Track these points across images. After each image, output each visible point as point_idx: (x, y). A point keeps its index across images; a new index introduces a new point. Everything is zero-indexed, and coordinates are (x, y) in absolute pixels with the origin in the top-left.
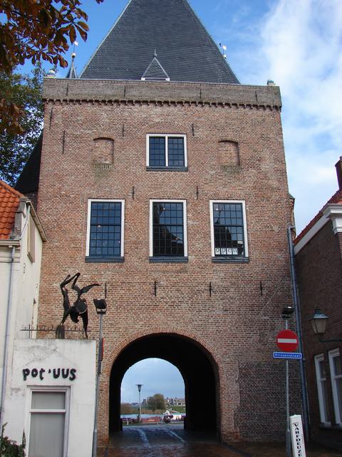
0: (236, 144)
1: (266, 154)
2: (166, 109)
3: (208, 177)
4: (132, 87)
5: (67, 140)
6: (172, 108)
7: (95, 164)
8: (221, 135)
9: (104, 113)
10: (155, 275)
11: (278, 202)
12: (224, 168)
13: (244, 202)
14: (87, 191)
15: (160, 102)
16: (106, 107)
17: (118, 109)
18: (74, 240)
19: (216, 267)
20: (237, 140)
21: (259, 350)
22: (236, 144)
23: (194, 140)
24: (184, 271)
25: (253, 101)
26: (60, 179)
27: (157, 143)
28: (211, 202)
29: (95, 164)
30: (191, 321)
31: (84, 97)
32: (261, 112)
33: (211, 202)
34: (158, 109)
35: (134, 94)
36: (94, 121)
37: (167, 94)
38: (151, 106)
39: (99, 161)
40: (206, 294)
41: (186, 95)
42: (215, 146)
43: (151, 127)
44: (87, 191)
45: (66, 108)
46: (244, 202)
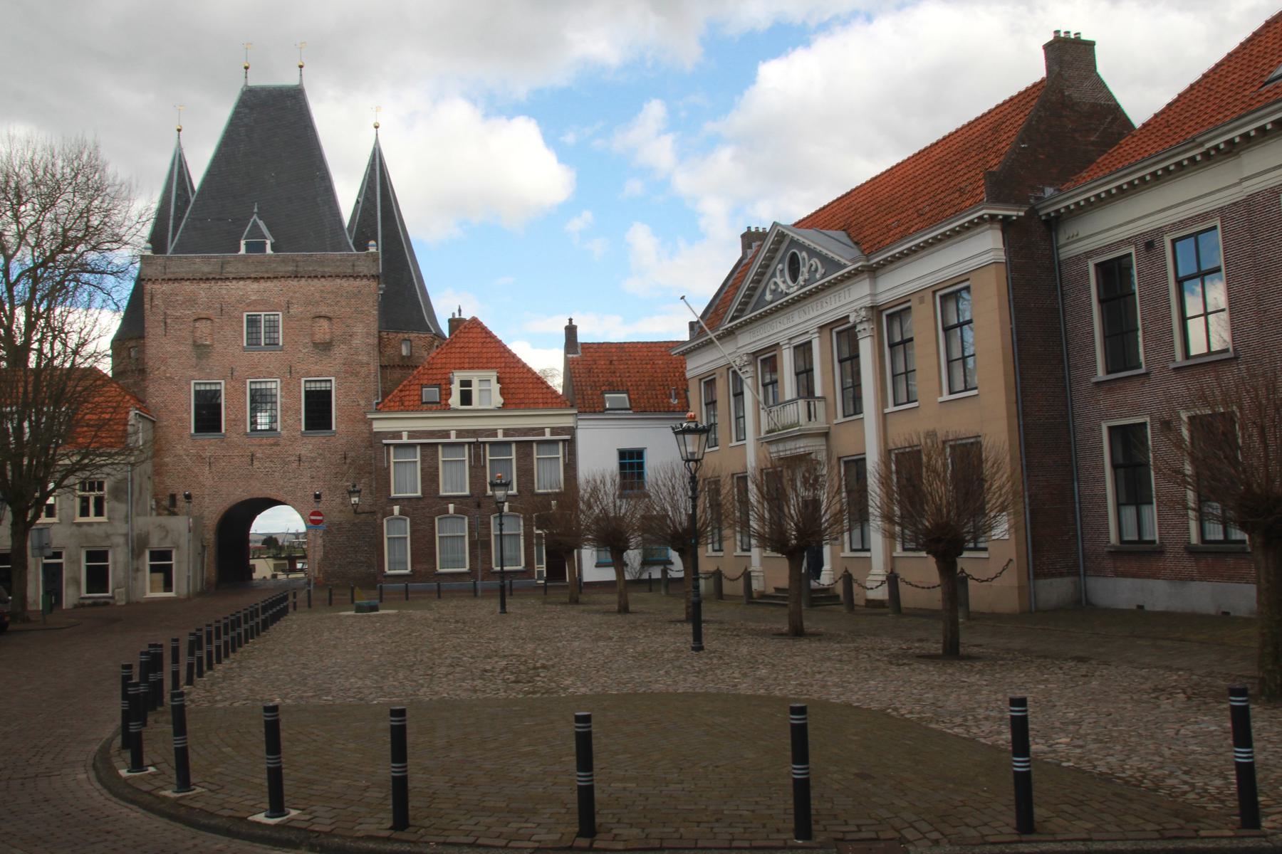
0: (330, 319)
1: (359, 329)
2: (263, 285)
3: (301, 355)
4: (229, 262)
5: (169, 321)
6: (269, 284)
7: (197, 346)
8: (315, 310)
9: (202, 290)
10: (252, 449)
11: (367, 376)
12: (316, 345)
13: (333, 379)
14: (190, 373)
15: (256, 279)
16: (203, 285)
17: (215, 287)
18: (180, 420)
19: (305, 440)
20: (331, 315)
21: (341, 511)
22: (330, 319)
23: (288, 318)
24: (276, 444)
25: (349, 271)
26: (164, 361)
27: (253, 322)
28: (303, 380)
29: (197, 346)
30: (283, 487)
31: (181, 276)
32: (358, 282)
33: (303, 380)
34: (255, 286)
35: (230, 270)
36: (191, 301)
37: (264, 269)
38: (248, 282)
39: (199, 342)
40: (295, 465)
41: (282, 269)
42: (309, 322)
43: (248, 305)
44: (190, 373)
45: (166, 287)
46: (333, 379)
